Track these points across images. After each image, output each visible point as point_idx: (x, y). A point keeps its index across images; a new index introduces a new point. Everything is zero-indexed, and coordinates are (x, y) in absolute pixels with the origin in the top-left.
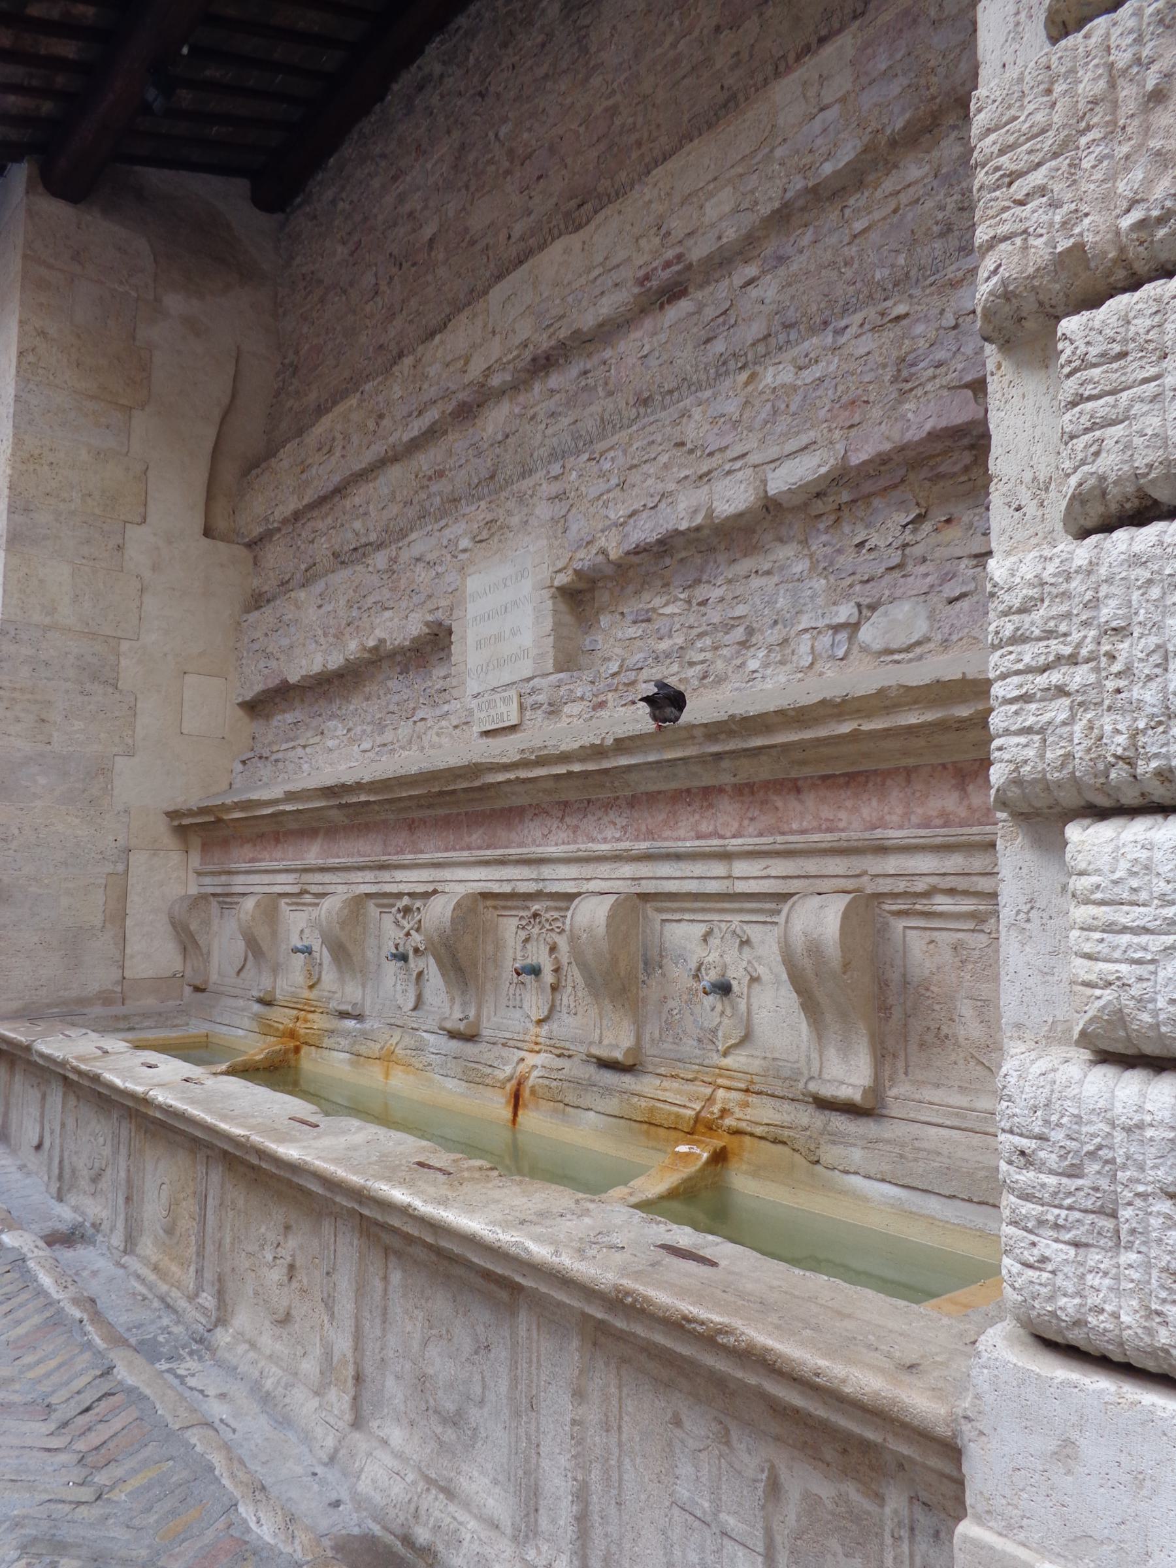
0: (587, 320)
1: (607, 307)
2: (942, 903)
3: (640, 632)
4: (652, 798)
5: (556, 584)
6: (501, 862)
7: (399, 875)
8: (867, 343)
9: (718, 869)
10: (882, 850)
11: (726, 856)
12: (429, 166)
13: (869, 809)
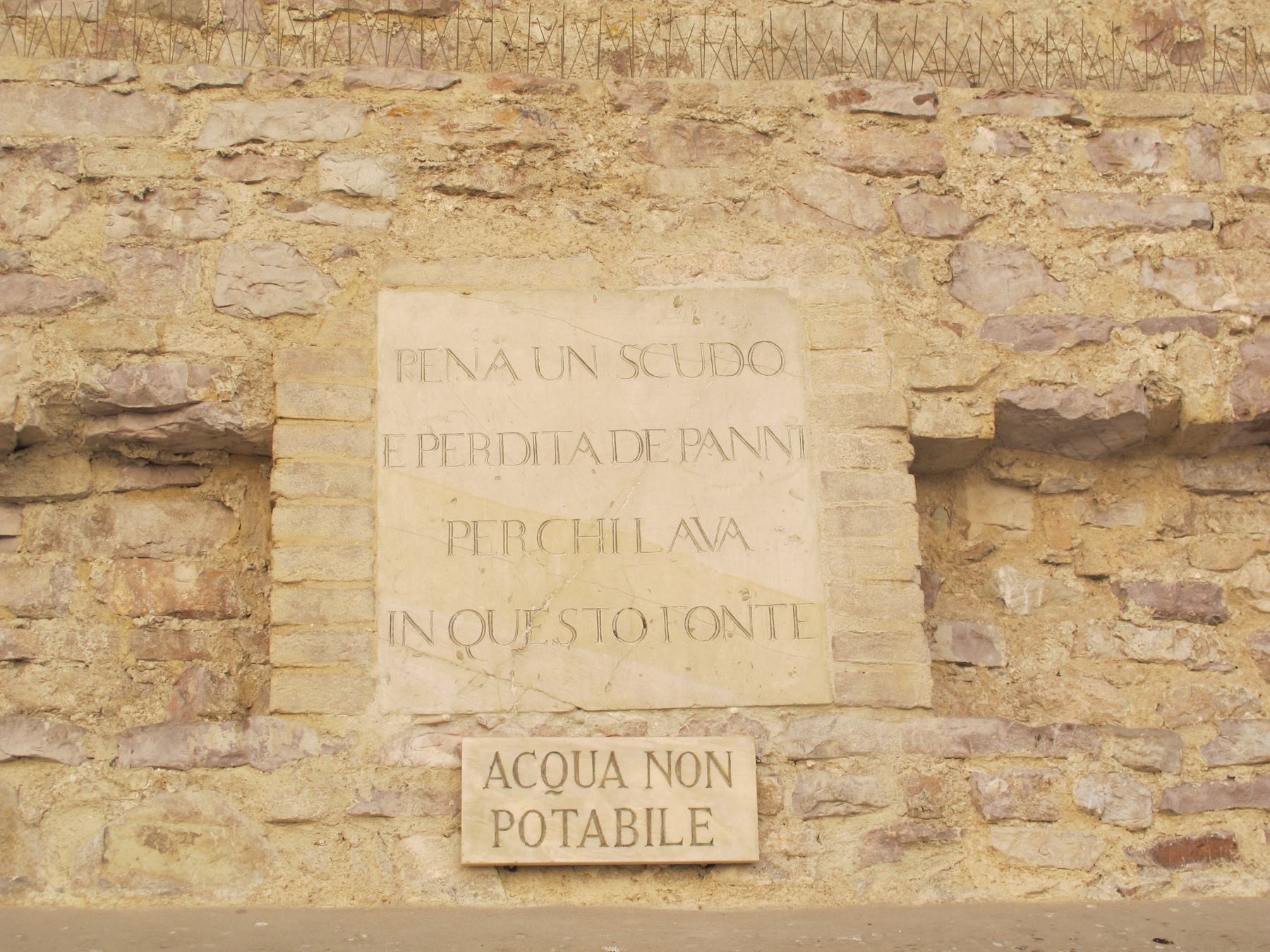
3: (1184, 650)
5: (923, 425)
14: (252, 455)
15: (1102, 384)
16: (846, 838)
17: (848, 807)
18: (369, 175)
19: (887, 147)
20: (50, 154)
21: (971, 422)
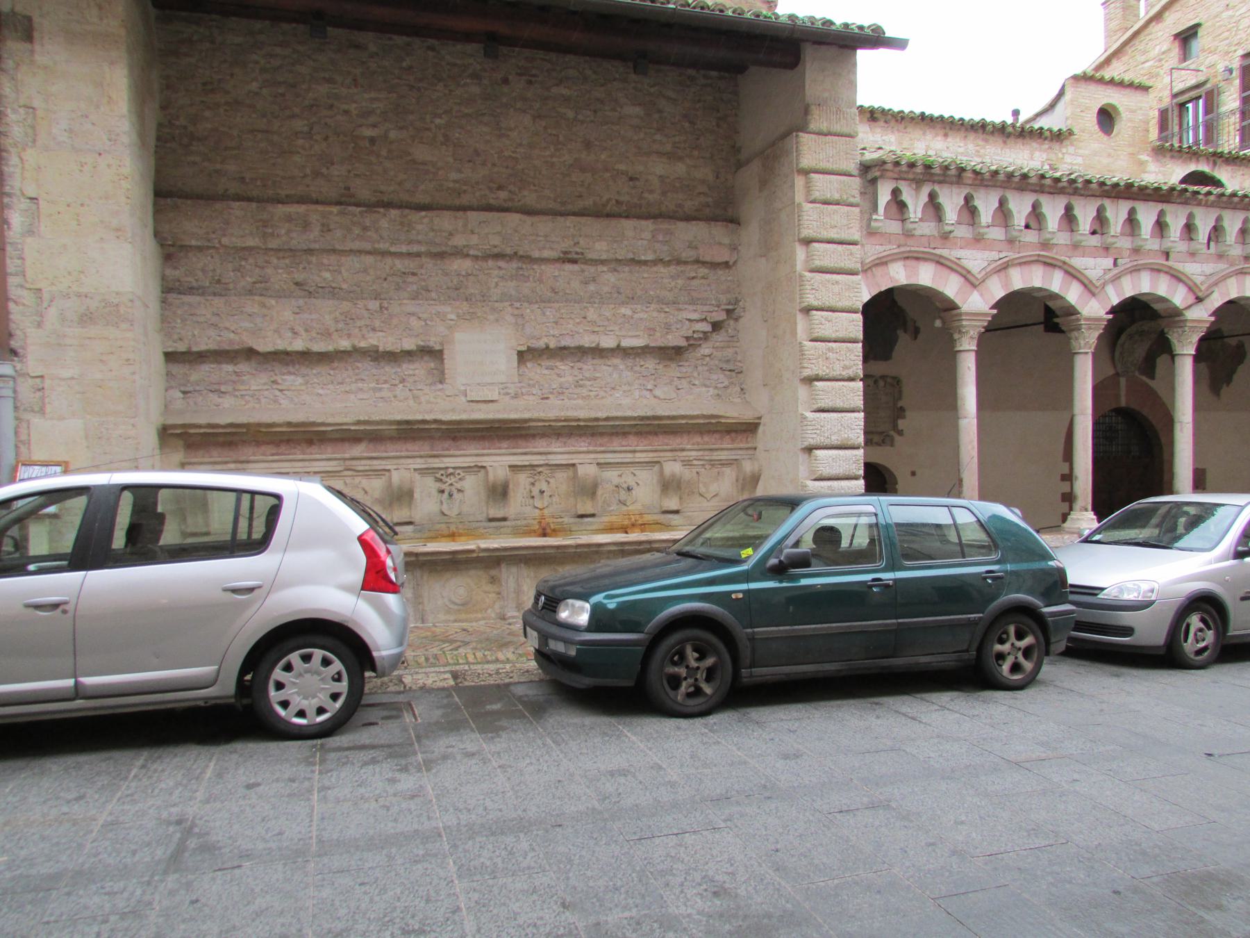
0: (536, 254)
1: (546, 254)
2: (695, 462)
4: (602, 434)
6: (525, 454)
7: (446, 460)
8: (655, 314)
9: (630, 455)
10: (683, 450)
11: (635, 452)
12: (366, 96)
13: (678, 440)
14: (441, 352)
15: (541, 344)
16: (507, 397)
17: (508, 394)
18: (453, 317)
19: (516, 312)
20: (413, 314)
21: (524, 348)
